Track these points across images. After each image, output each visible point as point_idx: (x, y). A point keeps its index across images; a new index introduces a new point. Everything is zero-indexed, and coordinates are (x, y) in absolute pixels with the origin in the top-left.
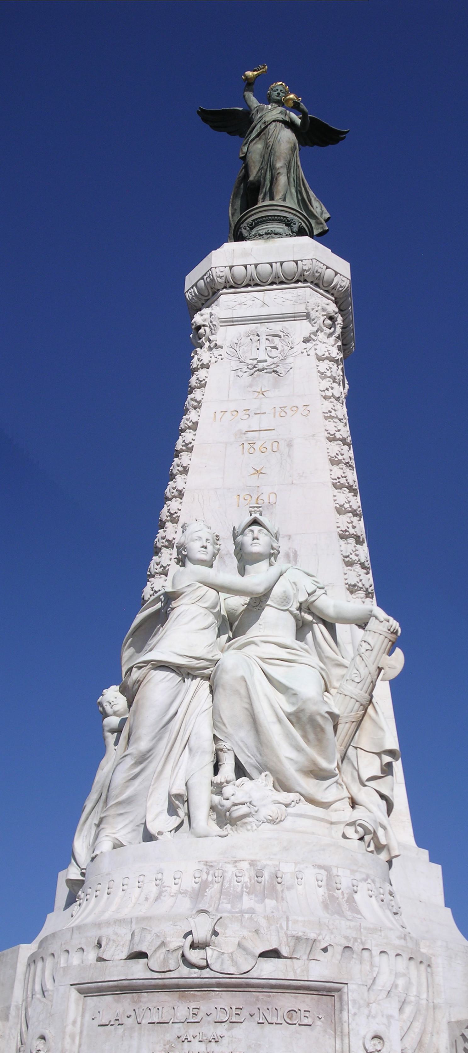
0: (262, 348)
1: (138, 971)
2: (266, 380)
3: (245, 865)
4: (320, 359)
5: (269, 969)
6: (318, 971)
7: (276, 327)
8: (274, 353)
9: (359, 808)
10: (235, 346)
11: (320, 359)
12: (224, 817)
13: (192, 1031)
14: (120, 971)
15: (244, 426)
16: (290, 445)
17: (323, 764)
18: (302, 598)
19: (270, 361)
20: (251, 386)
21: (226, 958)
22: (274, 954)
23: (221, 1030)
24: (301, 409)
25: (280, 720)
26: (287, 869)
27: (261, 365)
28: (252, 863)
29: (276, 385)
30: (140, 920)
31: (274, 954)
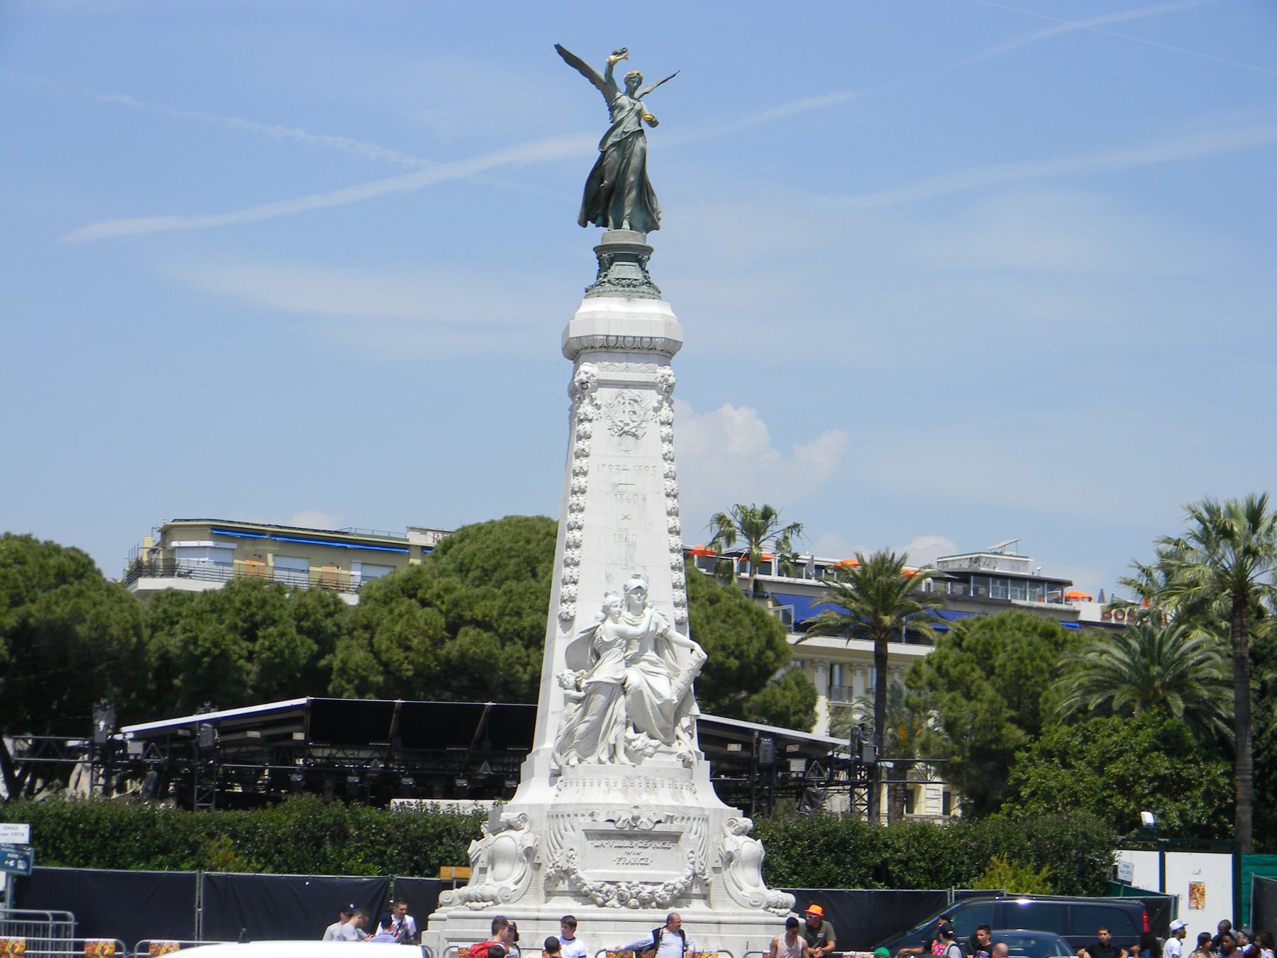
1: (611, 826)
4: (662, 423)
5: (659, 828)
6: (673, 827)
7: (635, 393)
8: (634, 418)
10: (610, 405)
11: (662, 423)
12: (635, 755)
14: (602, 825)
15: (616, 479)
16: (645, 500)
18: (659, 631)
19: (632, 425)
21: (645, 824)
22: (659, 822)
25: (653, 707)
26: (658, 779)
27: (626, 428)
31: (659, 822)
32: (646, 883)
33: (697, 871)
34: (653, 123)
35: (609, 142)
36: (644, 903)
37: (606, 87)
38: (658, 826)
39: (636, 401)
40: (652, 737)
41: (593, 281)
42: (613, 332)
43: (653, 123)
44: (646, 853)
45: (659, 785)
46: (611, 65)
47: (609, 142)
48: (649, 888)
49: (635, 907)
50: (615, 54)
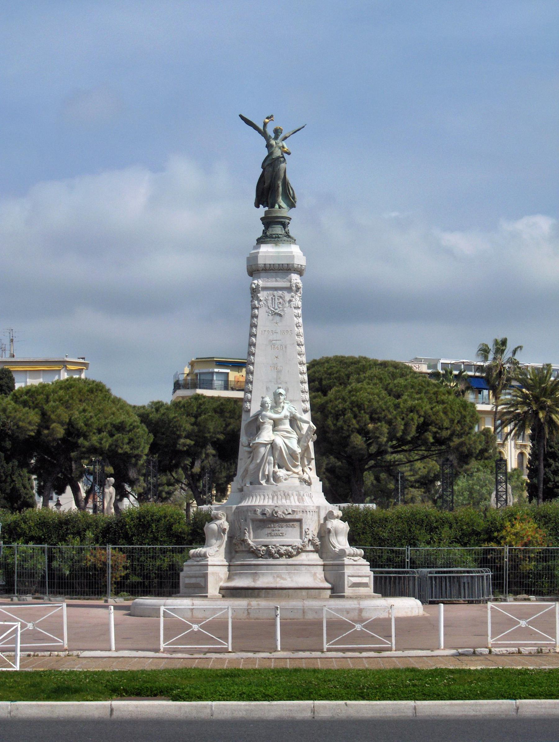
0: (276, 303)
2: (278, 318)
3: (282, 492)
5: (289, 517)
6: (297, 517)
9: (305, 473)
13: (275, 529)
15: (271, 338)
16: (286, 347)
17: (297, 463)
20: (273, 320)
22: (290, 514)
23: (280, 529)
24: (289, 332)
26: (290, 492)
28: (283, 491)
29: (281, 321)
30: (263, 506)
32: (283, 546)
33: (311, 539)
34: (289, 154)
35: (266, 164)
36: (281, 555)
37: (263, 133)
38: (289, 515)
39: (281, 297)
40: (287, 470)
41: (260, 234)
42: (268, 262)
43: (289, 154)
44: (283, 530)
45: (291, 495)
46: (265, 124)
47: (266, 164)
48: (285, 548)
49: (277, 558)
50: (268, 118)
